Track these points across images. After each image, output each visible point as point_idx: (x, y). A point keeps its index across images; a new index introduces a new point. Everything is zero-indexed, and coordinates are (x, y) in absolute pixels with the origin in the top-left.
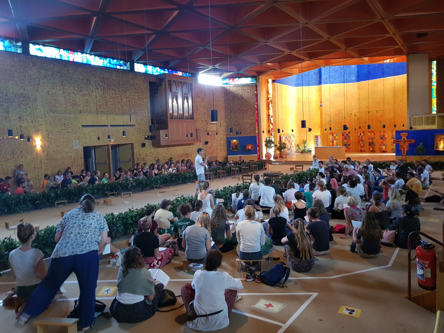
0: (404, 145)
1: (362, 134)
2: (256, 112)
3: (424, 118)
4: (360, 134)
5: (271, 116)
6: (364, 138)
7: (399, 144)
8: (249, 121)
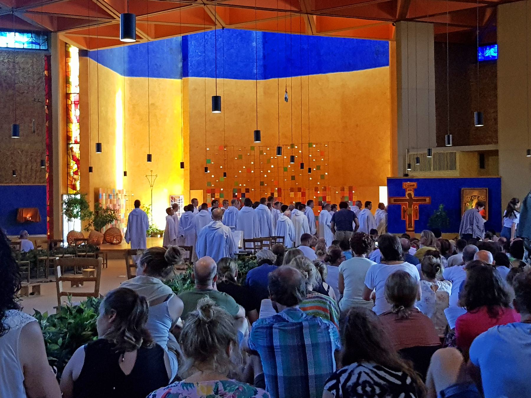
2: (47, 124)
8: (27, 146)
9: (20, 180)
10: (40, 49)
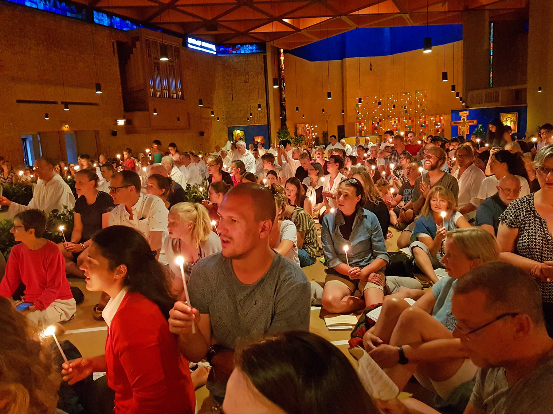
4: (395, 122)
6: (399, 127)
7: (457, 126)
9: (255, 122)
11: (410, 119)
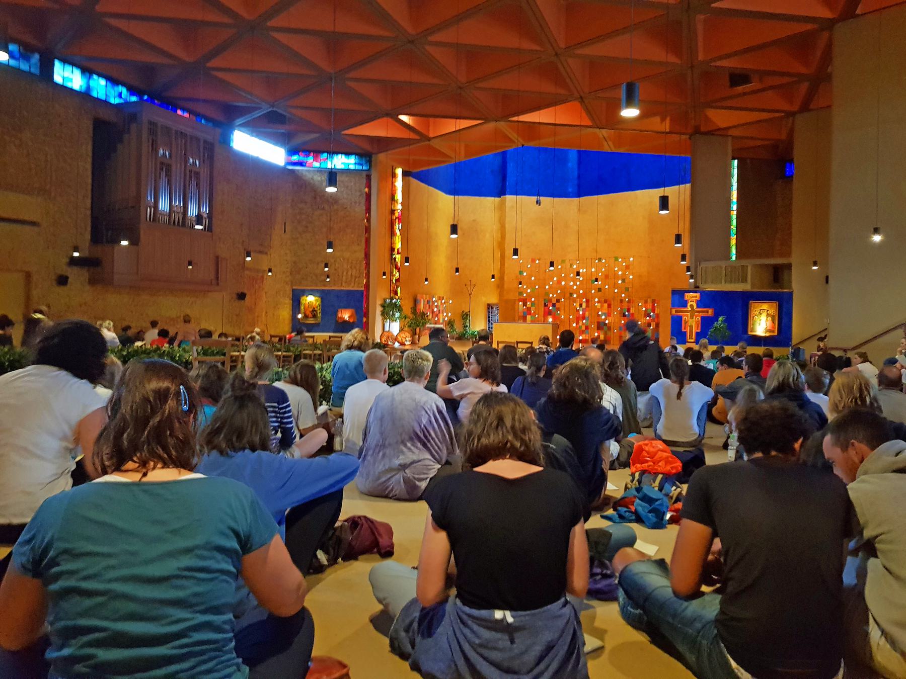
0: (691, 320)
1: (584, 305)
3: (723, 269)
4: (581, 305)
5: (396, 250)
6: (587, 314)
7: (681, 317)
8: (347, 255)
9: (342, 284)
10: (362, 170)
11: (606, 301)
